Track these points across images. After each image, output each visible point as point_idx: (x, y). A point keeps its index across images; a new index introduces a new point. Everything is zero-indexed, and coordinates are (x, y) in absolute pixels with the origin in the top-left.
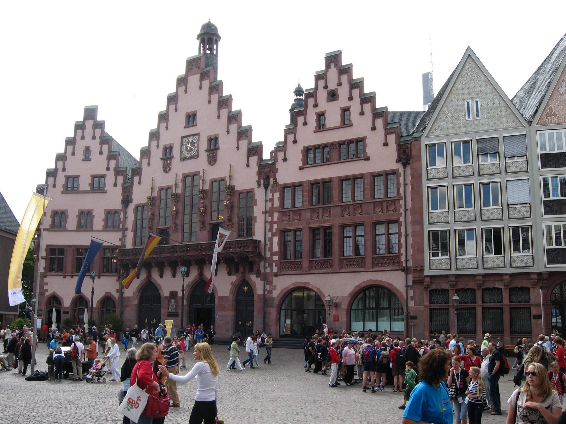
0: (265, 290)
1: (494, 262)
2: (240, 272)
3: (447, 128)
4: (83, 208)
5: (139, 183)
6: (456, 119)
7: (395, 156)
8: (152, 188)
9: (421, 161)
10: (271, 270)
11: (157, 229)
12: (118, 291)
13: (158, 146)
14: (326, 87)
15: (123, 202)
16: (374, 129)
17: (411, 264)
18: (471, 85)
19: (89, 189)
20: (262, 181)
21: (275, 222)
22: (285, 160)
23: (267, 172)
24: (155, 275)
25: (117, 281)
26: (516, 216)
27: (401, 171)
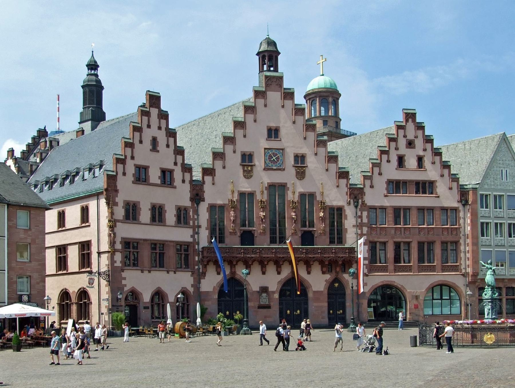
4: (155, 201)
7: (457, 197)
11: (241, 230)
12: (192, 286)
13: (234, 152)
15: (192, 199)
16: (442, 176)
19: (159, 182)
20: (352, 201)
22: (372, 187)
25: (191, 276)
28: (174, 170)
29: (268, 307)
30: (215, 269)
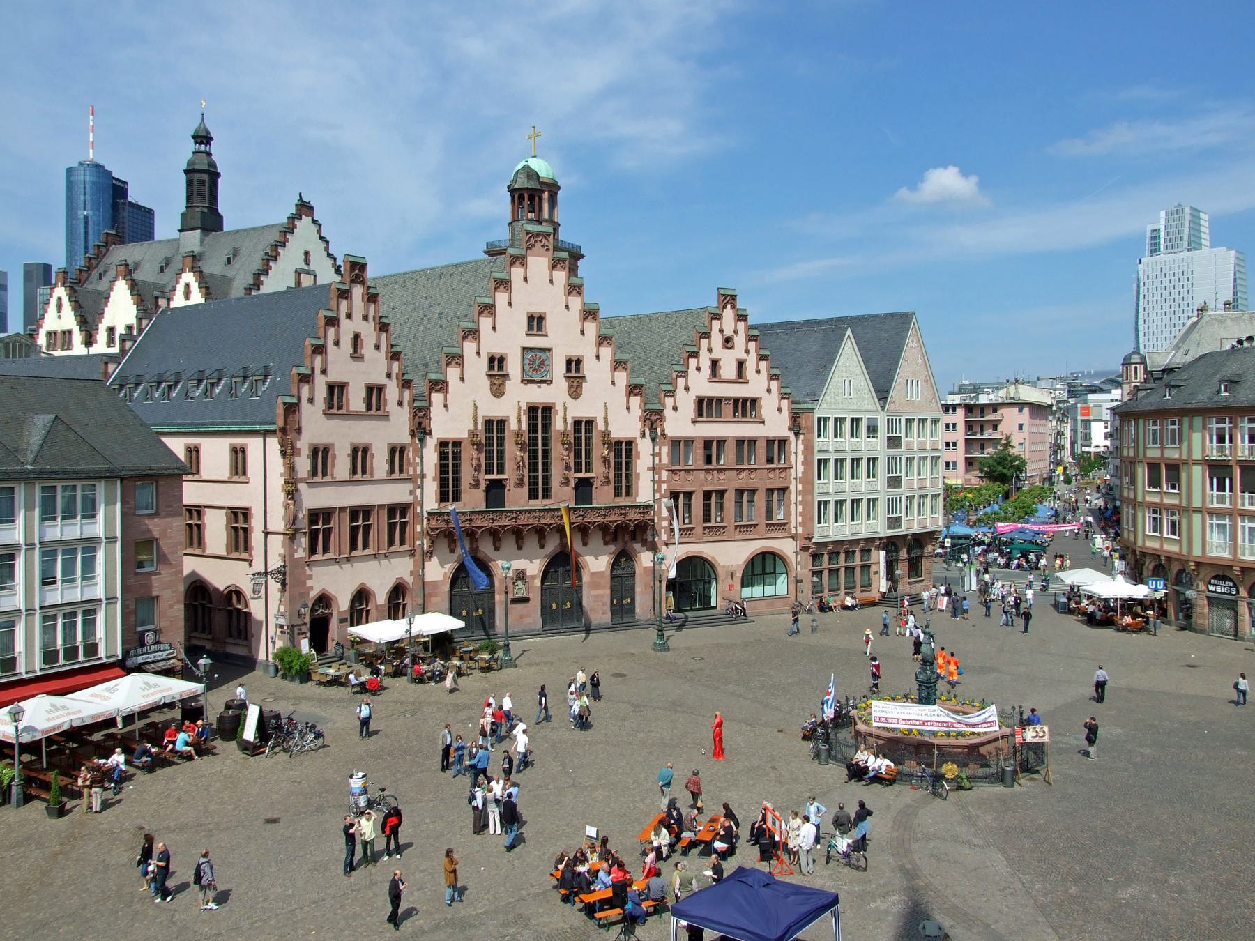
2: (620, 541)
13: (478, 354)
14: (721, 331)
16: (769, 391)
17: (800, 530)
22: (675, 408)
23: (652, 419)
24: (486, 548)
29: (526, 600)
30: (446, 545)
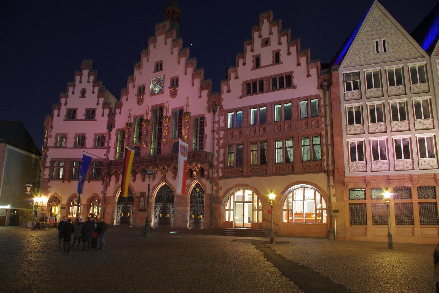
0: (212, 190)
1: (404, 165)
3: (360, 61)
5: (120, 113)
6: (367, 54)
8: (130, 117)
9: (339, 86)
10: (218, 175)
12: (102, 192)
13: (134, 87)
14: (260, 37)
16: (299, 64)
18: (379, 28)
19: (84, 118)
20: (211, 108)
21: (221, 139)
22: (229, 91)
25: (102, 185)
26: (421, 128)
27: (322, 96)
28: (96, 109)
